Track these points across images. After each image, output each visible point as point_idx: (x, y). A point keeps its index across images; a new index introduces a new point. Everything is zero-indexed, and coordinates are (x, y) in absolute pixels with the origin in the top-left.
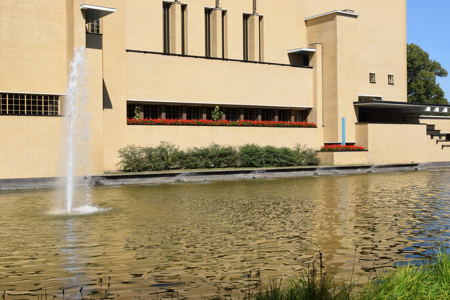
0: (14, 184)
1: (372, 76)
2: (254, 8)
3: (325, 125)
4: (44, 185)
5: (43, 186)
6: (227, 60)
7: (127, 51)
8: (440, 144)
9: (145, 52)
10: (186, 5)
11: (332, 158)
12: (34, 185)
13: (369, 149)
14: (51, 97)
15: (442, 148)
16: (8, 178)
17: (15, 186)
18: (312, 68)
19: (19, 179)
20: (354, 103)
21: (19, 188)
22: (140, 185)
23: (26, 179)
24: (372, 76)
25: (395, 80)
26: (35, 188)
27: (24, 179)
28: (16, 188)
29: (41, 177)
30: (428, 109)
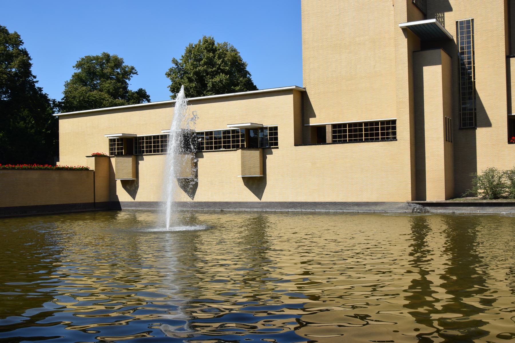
0: (340, 207)
4: (366, 209)
5: (366, 210)
12: (357, 209)
14: (388, 122)
16: (335, 201)
17: (341, 209)
19: (344, 202)
21: (344, 211)
22: (476, 214)
23: (350, 202)
26: (359, 211)
27: (348, 202)
28: (341, 211)
29: (363, 201)
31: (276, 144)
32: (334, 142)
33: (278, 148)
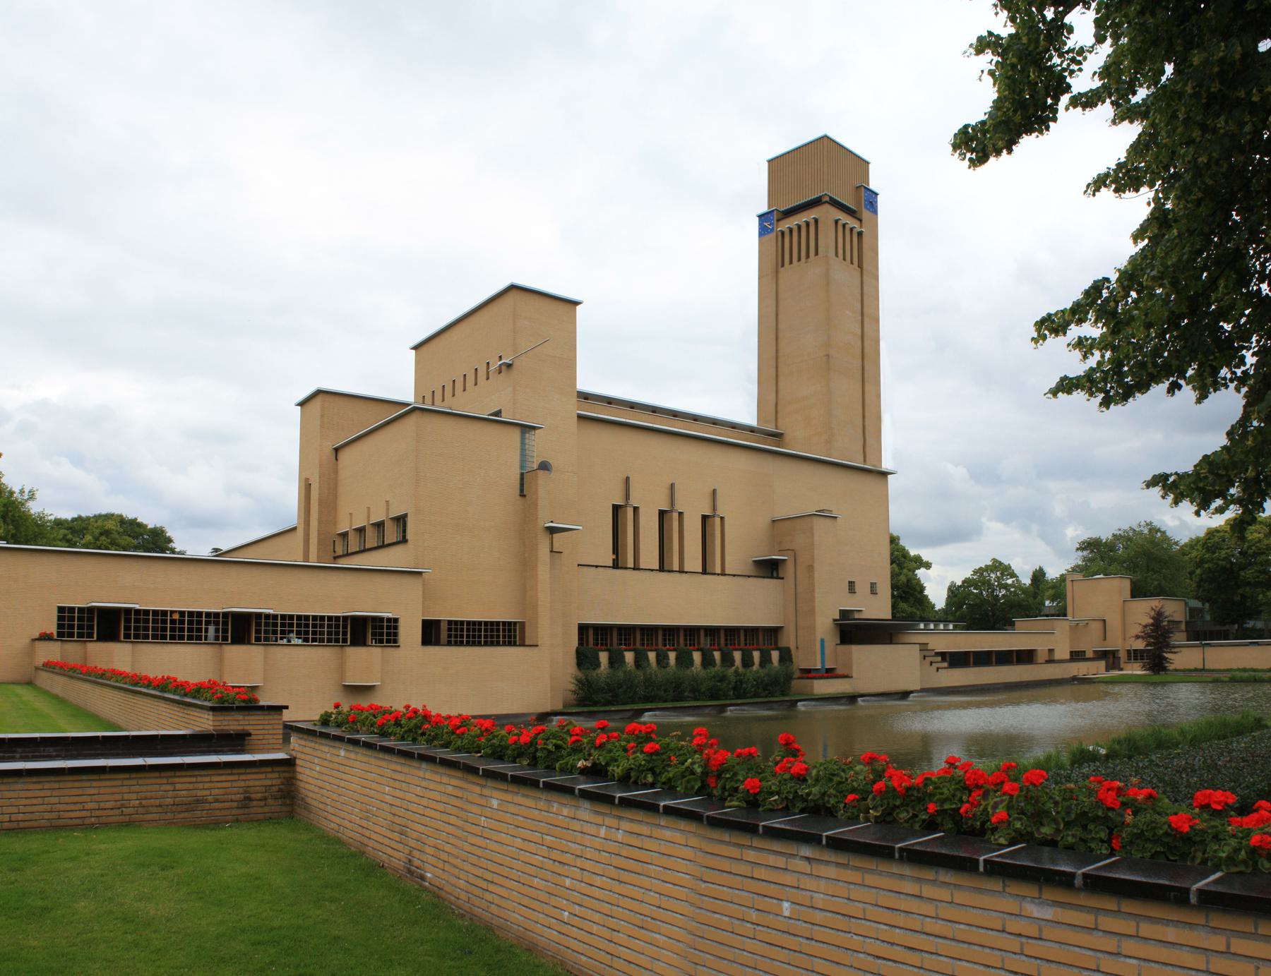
1: (851, 584)
2: (714, 508)
3: (799, 647)
6: (686, 572)
7: (579, 565)
8: (935, 666)
9: (597, 567)
10: (638, 507)
11: (812, 687)
13: (854, 675)
15: (938, 671)
18: (782, 578)
20: (835, 620)
24: (851, 584)
25: (879, 590)
30: (922, 626)
31: (395, 641)
32: (449, 643)
33: (399, 646)
